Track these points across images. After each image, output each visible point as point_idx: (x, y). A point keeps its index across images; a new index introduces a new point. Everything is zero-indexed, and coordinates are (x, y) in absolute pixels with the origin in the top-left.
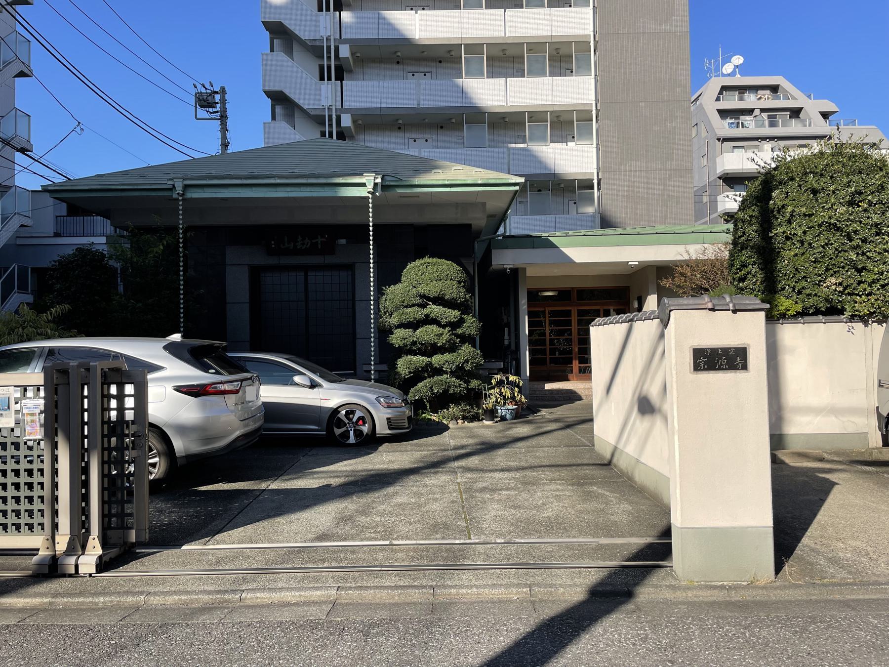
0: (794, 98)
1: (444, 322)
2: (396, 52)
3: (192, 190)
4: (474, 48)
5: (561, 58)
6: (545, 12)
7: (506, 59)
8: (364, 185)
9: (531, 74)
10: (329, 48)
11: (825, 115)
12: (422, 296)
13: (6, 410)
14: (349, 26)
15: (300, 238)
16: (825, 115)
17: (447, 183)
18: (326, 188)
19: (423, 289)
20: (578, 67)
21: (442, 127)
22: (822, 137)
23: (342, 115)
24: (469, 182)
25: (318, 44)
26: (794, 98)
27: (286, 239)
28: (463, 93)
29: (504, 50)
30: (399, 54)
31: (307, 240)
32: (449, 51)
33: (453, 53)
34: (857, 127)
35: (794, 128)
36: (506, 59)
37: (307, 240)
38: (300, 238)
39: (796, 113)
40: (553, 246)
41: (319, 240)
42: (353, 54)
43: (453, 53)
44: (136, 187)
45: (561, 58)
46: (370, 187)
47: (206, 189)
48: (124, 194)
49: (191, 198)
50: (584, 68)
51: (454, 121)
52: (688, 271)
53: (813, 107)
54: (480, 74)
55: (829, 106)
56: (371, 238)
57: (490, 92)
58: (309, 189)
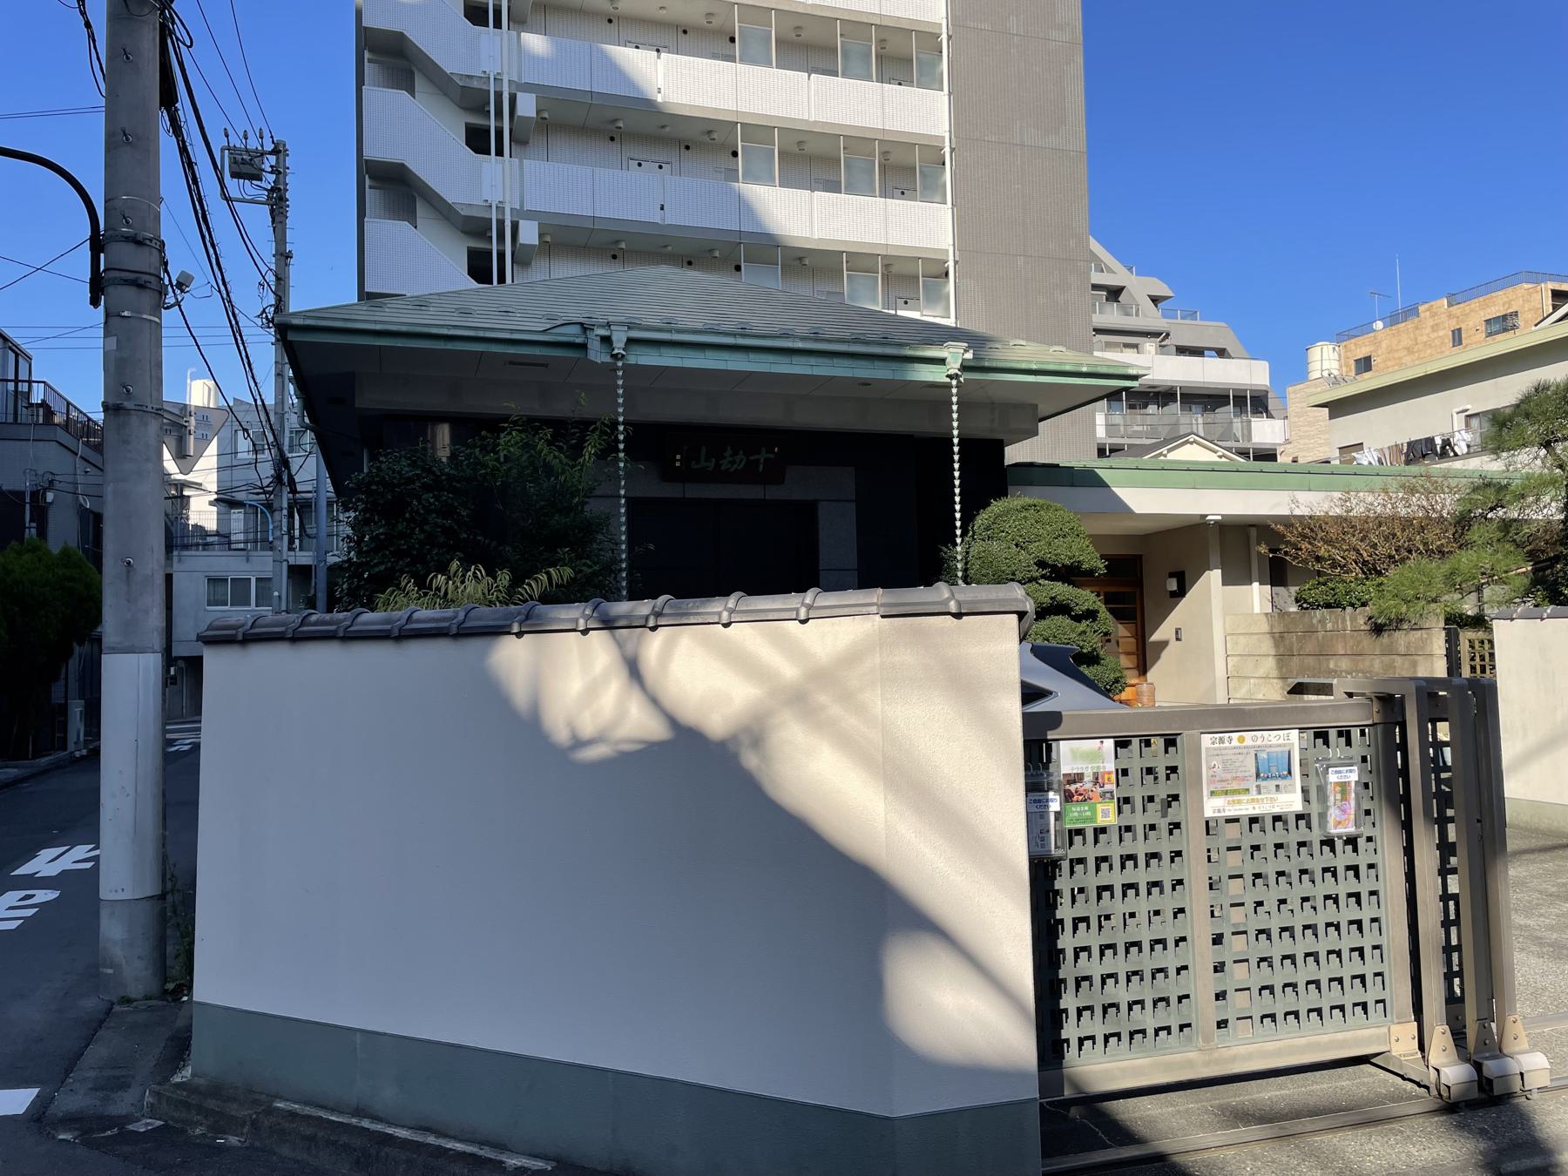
0: (1110, 271)
1: (1078, 610)
2: (615, 120)
3: (639, 350)
4: (758, 132)
5: (898, 168)
6: (872, 88)
7: (814, 159)
8: (942, 361)
9: (851, 190)
10: (499, 95)
11: (1155, 300)
12: (1041, 564)
13: (1284, 777)
14: (536, 60)
15: (729, 452)
16: (1155, 300)
17: (1034, 367)
18: (877, 364)
19: (1039, 549)
20: (925, 187)
21: (690, 263)
22: (1156, 334)
23: (522, 223)
24: (1068, 368)
25: (475, 84)
26: (1110, 271)
27: (704, 450)
28: (743, 207)
29: (800, 143)
30: (621, 124)
31: (741, 456)
32: (710, 132)
33: (715, 136)
34: (1198, 322)
35: (1111, 316)
36: (814, 159)
37: (741, 456)
38: (729, 452)
39: (1114, 293)
40: (1102, 484)
41: (763, 456)
42: (538, 112)
43: (715, 136)
44: (481, 334)
45: (898, 168)
46: (954, 366)
47: (664, 350)
48: (450, 346)
49: (637, 365)
50: (932, 191)
51: (717, 254)
52: (1333, 531)
53: (1139, 287)
54: (769, 181)
55: (1162, 289)
56: (956, 457)
57: (797, 214)
58: (847, 362)
